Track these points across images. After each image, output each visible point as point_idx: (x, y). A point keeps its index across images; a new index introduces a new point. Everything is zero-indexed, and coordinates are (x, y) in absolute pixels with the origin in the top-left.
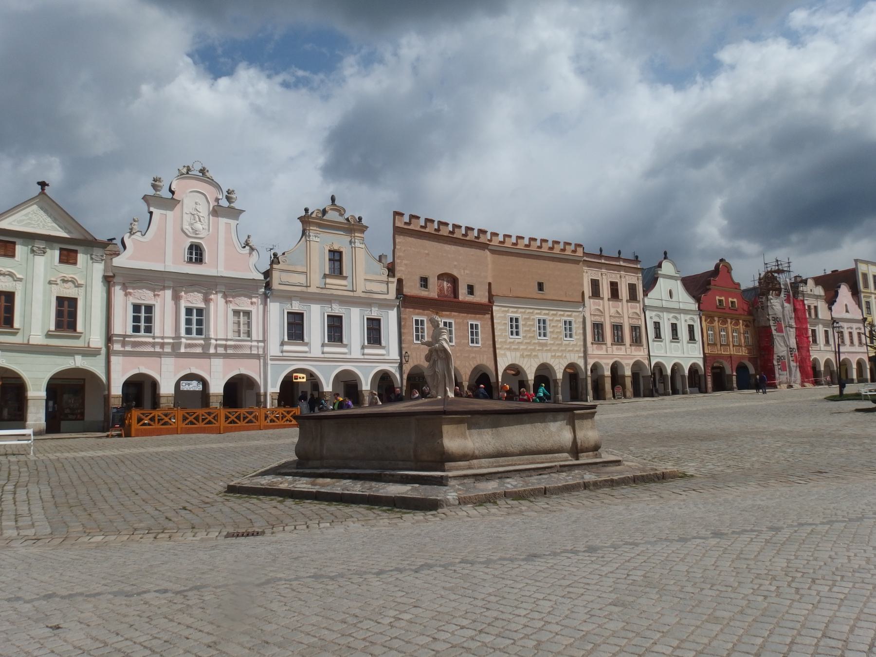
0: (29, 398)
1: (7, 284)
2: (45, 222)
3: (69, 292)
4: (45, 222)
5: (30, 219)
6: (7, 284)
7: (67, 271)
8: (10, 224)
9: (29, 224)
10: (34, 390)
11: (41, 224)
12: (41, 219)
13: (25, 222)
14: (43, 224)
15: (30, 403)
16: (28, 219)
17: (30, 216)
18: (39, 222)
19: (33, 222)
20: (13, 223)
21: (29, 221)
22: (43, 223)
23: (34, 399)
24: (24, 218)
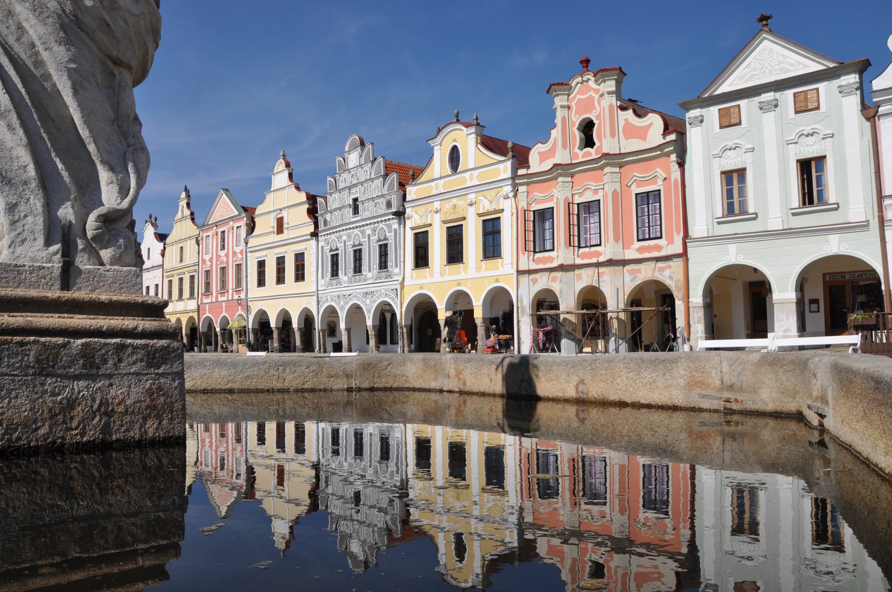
0: (774, 302)
1: (736, 160)
2: (771, 66)
3: (809, 150)
4: (771, 66)
5: (754, 69)
6: (736, 160)
7: (807, 121)
8: (731, 84)
9: (753, 75)
10: (779, 292)
11: (767, 71)
12: (766, 64)
13: (748, 76)
14: (770, 70)
15: (776, 308)
16: (751, 70)
17: (752, 66)
18: (764, 70)
19: (757, 72)
20: (735, 83)
21: (753, 73)
22: (769, 68)
23: (783, 302)
24: (746, 70)
